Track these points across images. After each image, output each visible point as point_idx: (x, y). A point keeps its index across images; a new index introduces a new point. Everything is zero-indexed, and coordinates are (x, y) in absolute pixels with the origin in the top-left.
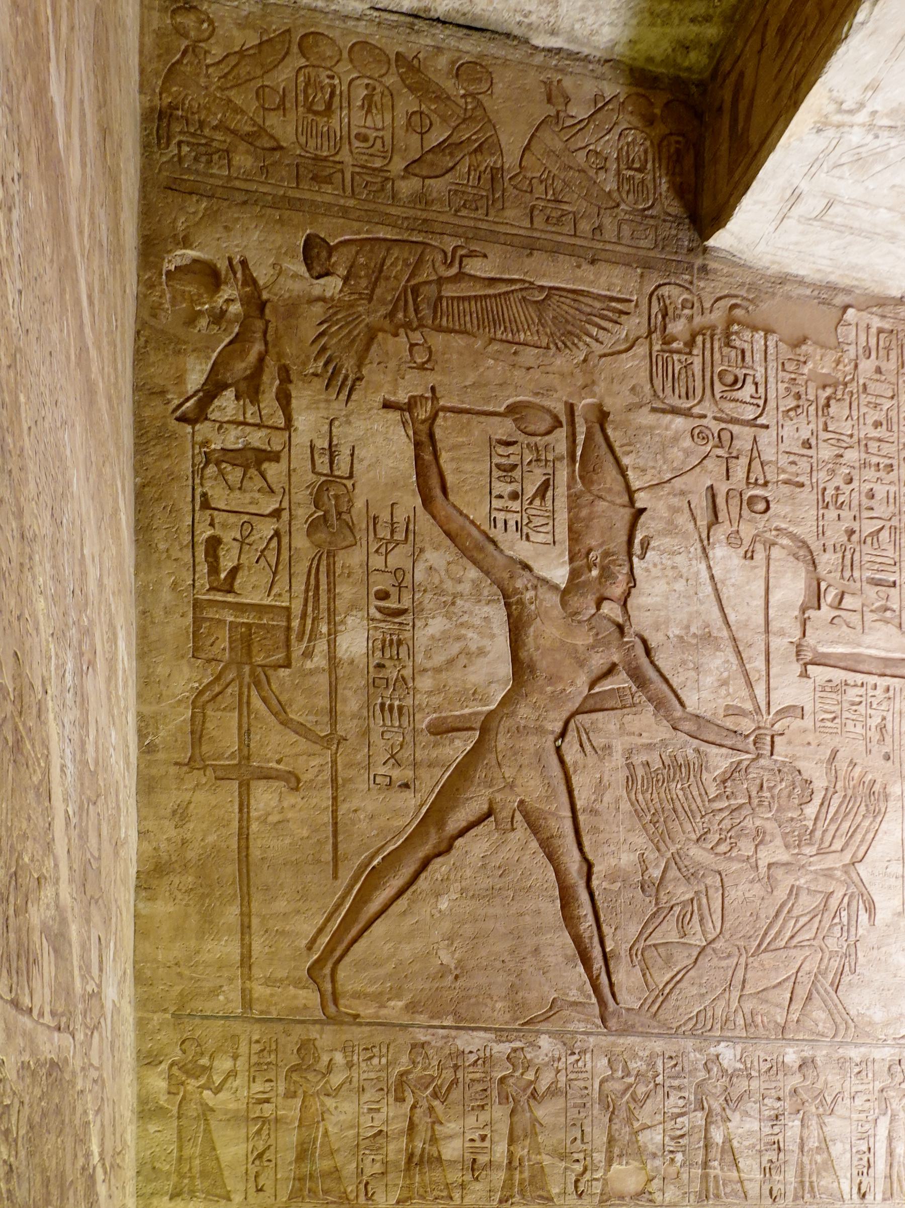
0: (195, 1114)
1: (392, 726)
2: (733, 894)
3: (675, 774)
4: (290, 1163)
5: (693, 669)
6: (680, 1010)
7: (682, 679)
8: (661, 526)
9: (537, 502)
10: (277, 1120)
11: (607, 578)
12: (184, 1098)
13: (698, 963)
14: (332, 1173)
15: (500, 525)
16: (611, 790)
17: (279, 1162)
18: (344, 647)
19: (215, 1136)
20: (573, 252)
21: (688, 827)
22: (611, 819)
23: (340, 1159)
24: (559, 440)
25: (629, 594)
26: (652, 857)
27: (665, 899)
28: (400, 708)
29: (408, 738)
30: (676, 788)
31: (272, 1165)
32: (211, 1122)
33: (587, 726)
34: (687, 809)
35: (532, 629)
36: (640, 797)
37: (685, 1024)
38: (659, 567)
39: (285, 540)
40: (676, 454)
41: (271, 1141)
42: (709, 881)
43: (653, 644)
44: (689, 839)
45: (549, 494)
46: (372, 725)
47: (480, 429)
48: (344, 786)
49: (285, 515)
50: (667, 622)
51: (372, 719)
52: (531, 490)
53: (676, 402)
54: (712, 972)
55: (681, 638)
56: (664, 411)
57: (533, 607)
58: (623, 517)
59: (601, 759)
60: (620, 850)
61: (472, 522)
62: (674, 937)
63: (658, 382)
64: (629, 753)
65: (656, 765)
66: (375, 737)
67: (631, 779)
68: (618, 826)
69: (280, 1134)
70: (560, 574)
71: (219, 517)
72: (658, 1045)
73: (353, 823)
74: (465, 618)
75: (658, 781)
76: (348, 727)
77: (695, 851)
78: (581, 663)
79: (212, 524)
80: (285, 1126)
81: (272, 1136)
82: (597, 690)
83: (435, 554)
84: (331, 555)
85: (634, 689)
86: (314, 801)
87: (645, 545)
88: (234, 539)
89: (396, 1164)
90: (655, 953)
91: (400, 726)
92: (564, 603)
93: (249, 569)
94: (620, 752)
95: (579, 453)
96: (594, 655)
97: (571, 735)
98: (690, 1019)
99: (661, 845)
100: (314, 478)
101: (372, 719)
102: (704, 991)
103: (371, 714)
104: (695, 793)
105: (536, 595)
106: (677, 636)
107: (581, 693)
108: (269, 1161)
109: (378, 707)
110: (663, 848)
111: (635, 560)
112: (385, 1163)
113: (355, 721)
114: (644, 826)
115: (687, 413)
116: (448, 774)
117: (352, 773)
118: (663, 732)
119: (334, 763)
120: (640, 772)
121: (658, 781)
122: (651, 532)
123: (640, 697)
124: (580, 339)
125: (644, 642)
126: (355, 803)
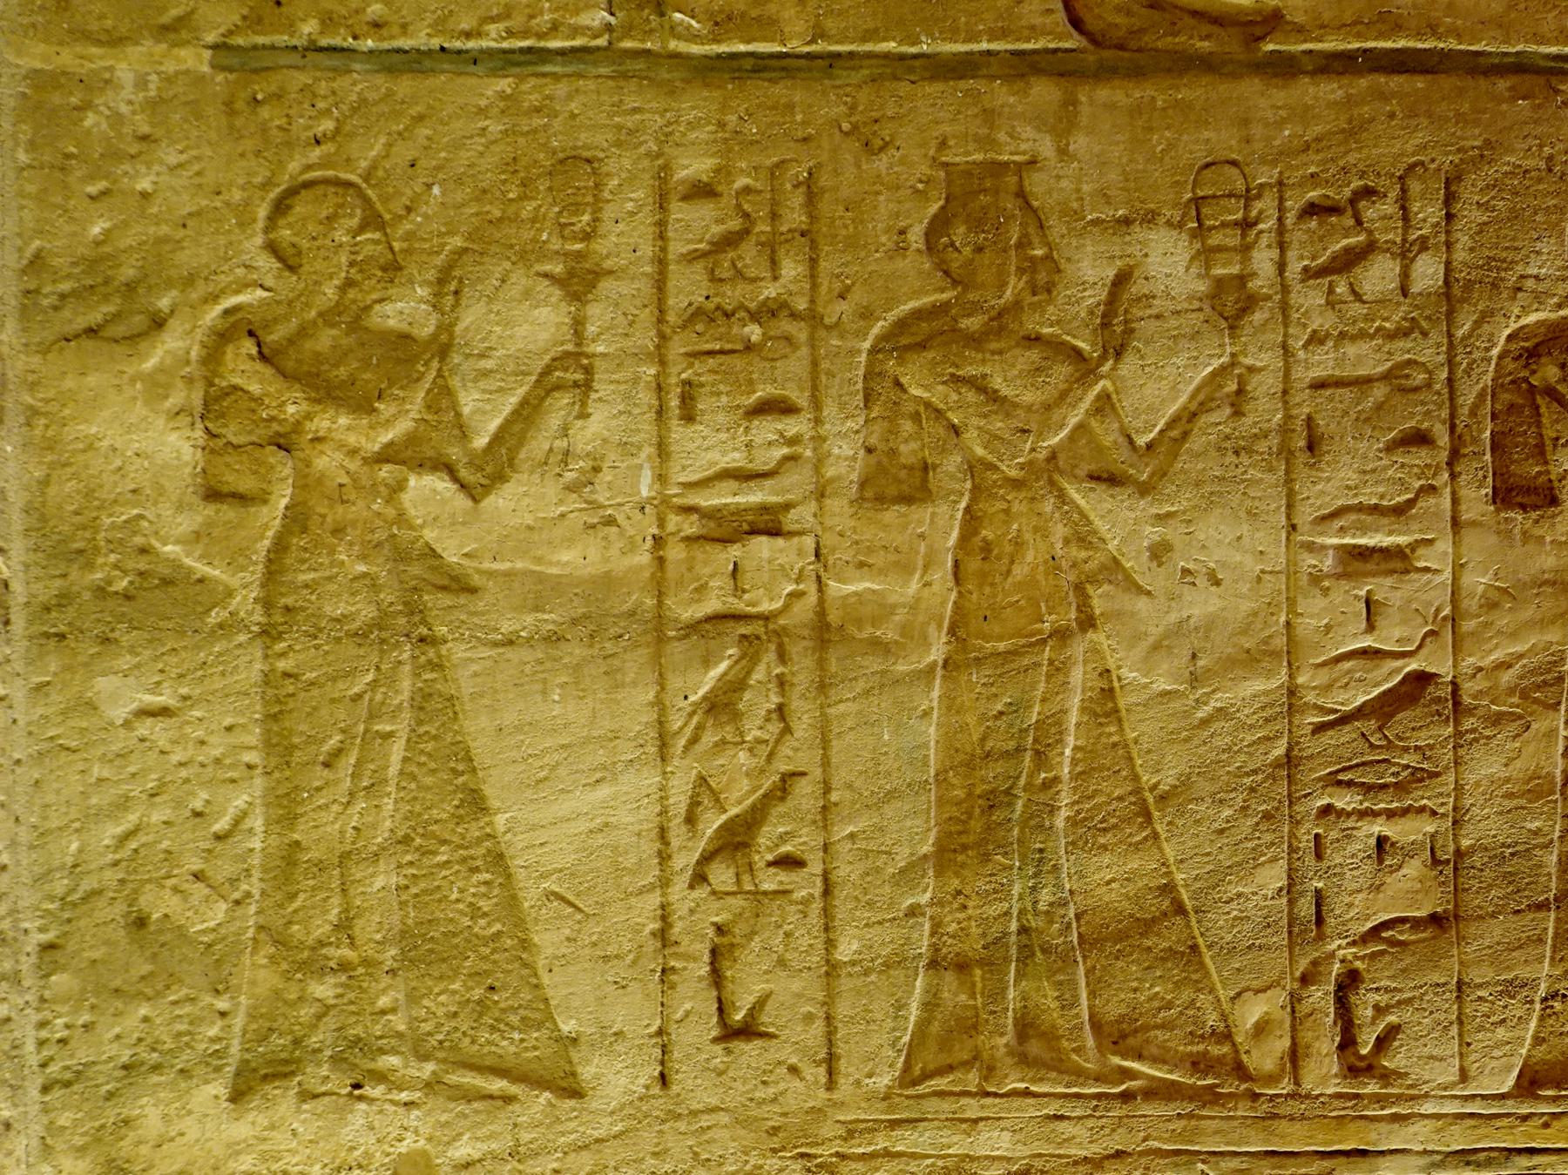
0: (368, 613)
4: (908, 876)
10: (823, 632)
12: (297, 518)
14: (1148, 926)
17: (844, 870)
19: (477, 729)
23: (1183, 852)
31: (805, 884)
32: (457, 651)
41: (798, 754)
69: (844, 709)
80: (874, 664)
81: (803, 726)
89: (1511, 858)
108: (790, 862)
112: (1450, 864)
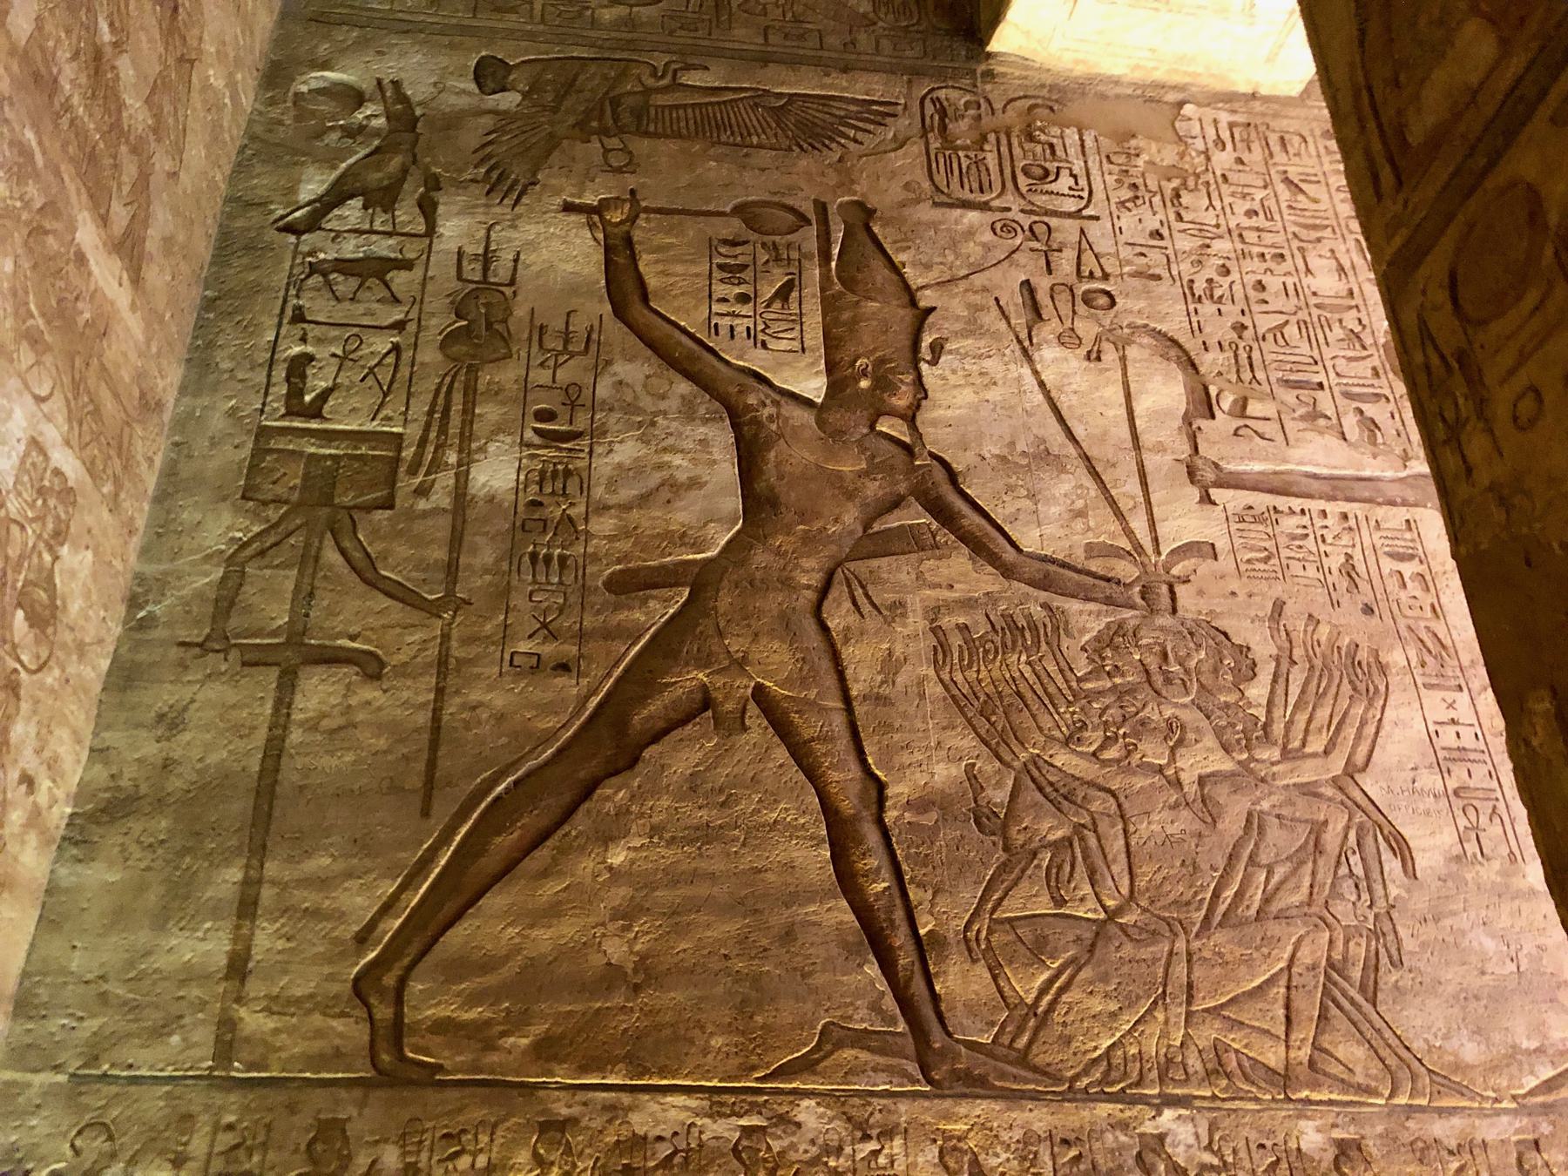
1: (549, 583)
2: (1144, 829)
3: (1014, 642)
5: (1027, 497)
6: (1074, 1045)
7: (1010, 509)
9: (777, 305)
11: (883, 390)
13: (1097, 953)
15: (724, 332)
16: (907, 668)
18: (482, 479)
20: (817, 63)
21: (1046, 722)
22: (912, 710)
24: (809, 238)
25: (918, 407)
26: (989, 768)
27: (1021, 839)
28: (563, 560)
29: (572, 599)
30: (1019, 662)
33: (862, 577)
34: (1040, 692)
35: (772, 454)
36: (959, 677)
37: (1086, 1072)
38: (961, 373)
39: (407, 355)
40: (972, 250)
42: (1095, 807)
44: (1053, 738)
45: (795, 294)
46: (515, 583)
47: (693, 229)
48: (458, 671)
49: (411, 327)
50: (980, 436)
51: (515, 575)
52: (768, 292)
54: (1125, 969)
55: (1002, 459)
57: (774, 427)
58: (902, 319)
59: (889, 622)
60: (930, 762)
61: (684, 331)
62: (1044, 906)
64: (934, 612)
65: (982, 629)
66: (518, 600)
67: (941, 649)
68: (925, 721)
70: (814, 386)
71: (313, 331)
72: (1039, 1118)
73: (467, 726)
74: (671, 441)
75: (986, 652)
76: (472, 584)
77: (1062, 759)
78: (850, 496)
79: (303, 340)
82: (876, 527)
83: (629, 367)
84: (473, 370)
85: (935, 526)
86: (405, 694)
87: (937, 349)
88: (334, 355)
90: (1012, 937)
91: (561, 583)
92: (821, 423)
93: (349, 389)
94: (920, 612)
95: (836, 251)
96: (869, 484)
97: (838, 591)
98: (1095, 1061)
99: (1003, 750)
100: (455, 285)
101: (515, 575)
102: (1113, 1006)
103: (514, 568)
104: (1052, 668)
105: (778, 415)
106: (997, 456)
107: (851, 533)
109: (526, 559)
110: (1008, 757)
111: (924, 367)
113: (488, 578)
114: (969, 721)
116: (637, 648)
117: (474, 651)
118: (986, 581)
119: (446, 637)
120: (956, 641)
121: (986, 652)
122: (945, 334)
123: (946, 536)
124: (832, 140)
126: (475, 696)
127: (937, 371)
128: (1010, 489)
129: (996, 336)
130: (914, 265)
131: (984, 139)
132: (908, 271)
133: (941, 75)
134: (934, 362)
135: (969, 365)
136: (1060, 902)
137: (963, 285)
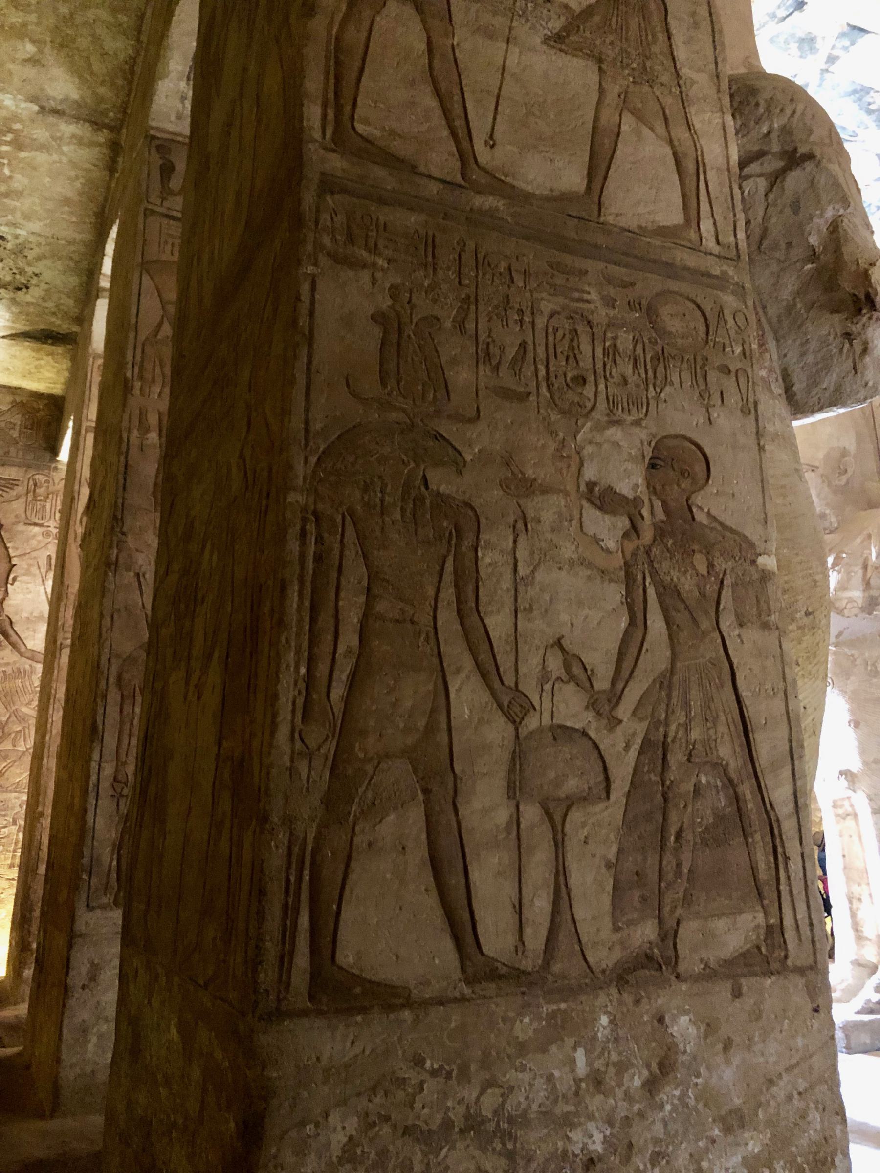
7: (27, 634)
8: (23, 572)
30: (19, 682)
40: (34, 543)
43: (13, 620)
50: (22, 611)
53: (37, 521)
55: (28, 618)
56: (30, 524)
62: (10, 747)
63: (29, 513)
115: (41, 525)
125: (10, 619)
127: (13, 587)
128: (28, 628)
129: (34, 575)
130: (13, 548)
131: (48, 497)
132: (10, 550)
133: (38, 468)
134: (12, 584)
135: (24, 586)
136: (14, 746)
137: (27, 556)
